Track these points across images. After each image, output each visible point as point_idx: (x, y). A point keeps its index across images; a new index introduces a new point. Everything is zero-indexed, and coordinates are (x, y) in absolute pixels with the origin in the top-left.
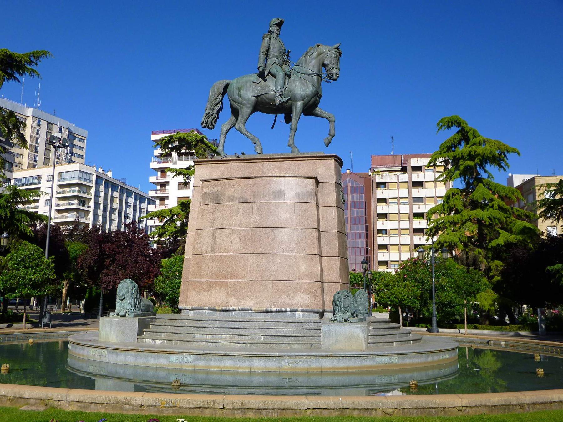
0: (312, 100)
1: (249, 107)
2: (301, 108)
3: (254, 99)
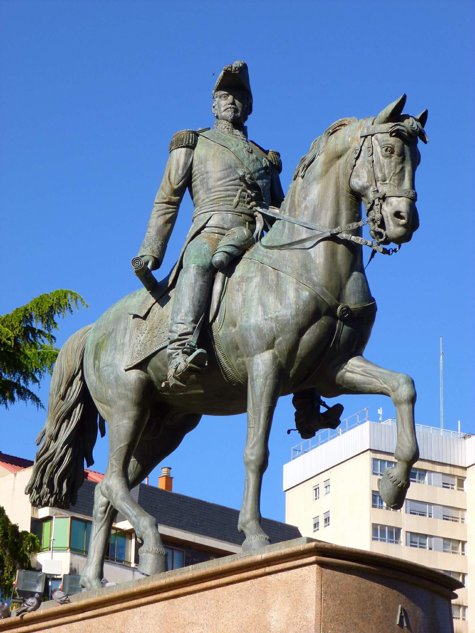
0: (306, 337)
1: (124, 410)
2: (266, 379)
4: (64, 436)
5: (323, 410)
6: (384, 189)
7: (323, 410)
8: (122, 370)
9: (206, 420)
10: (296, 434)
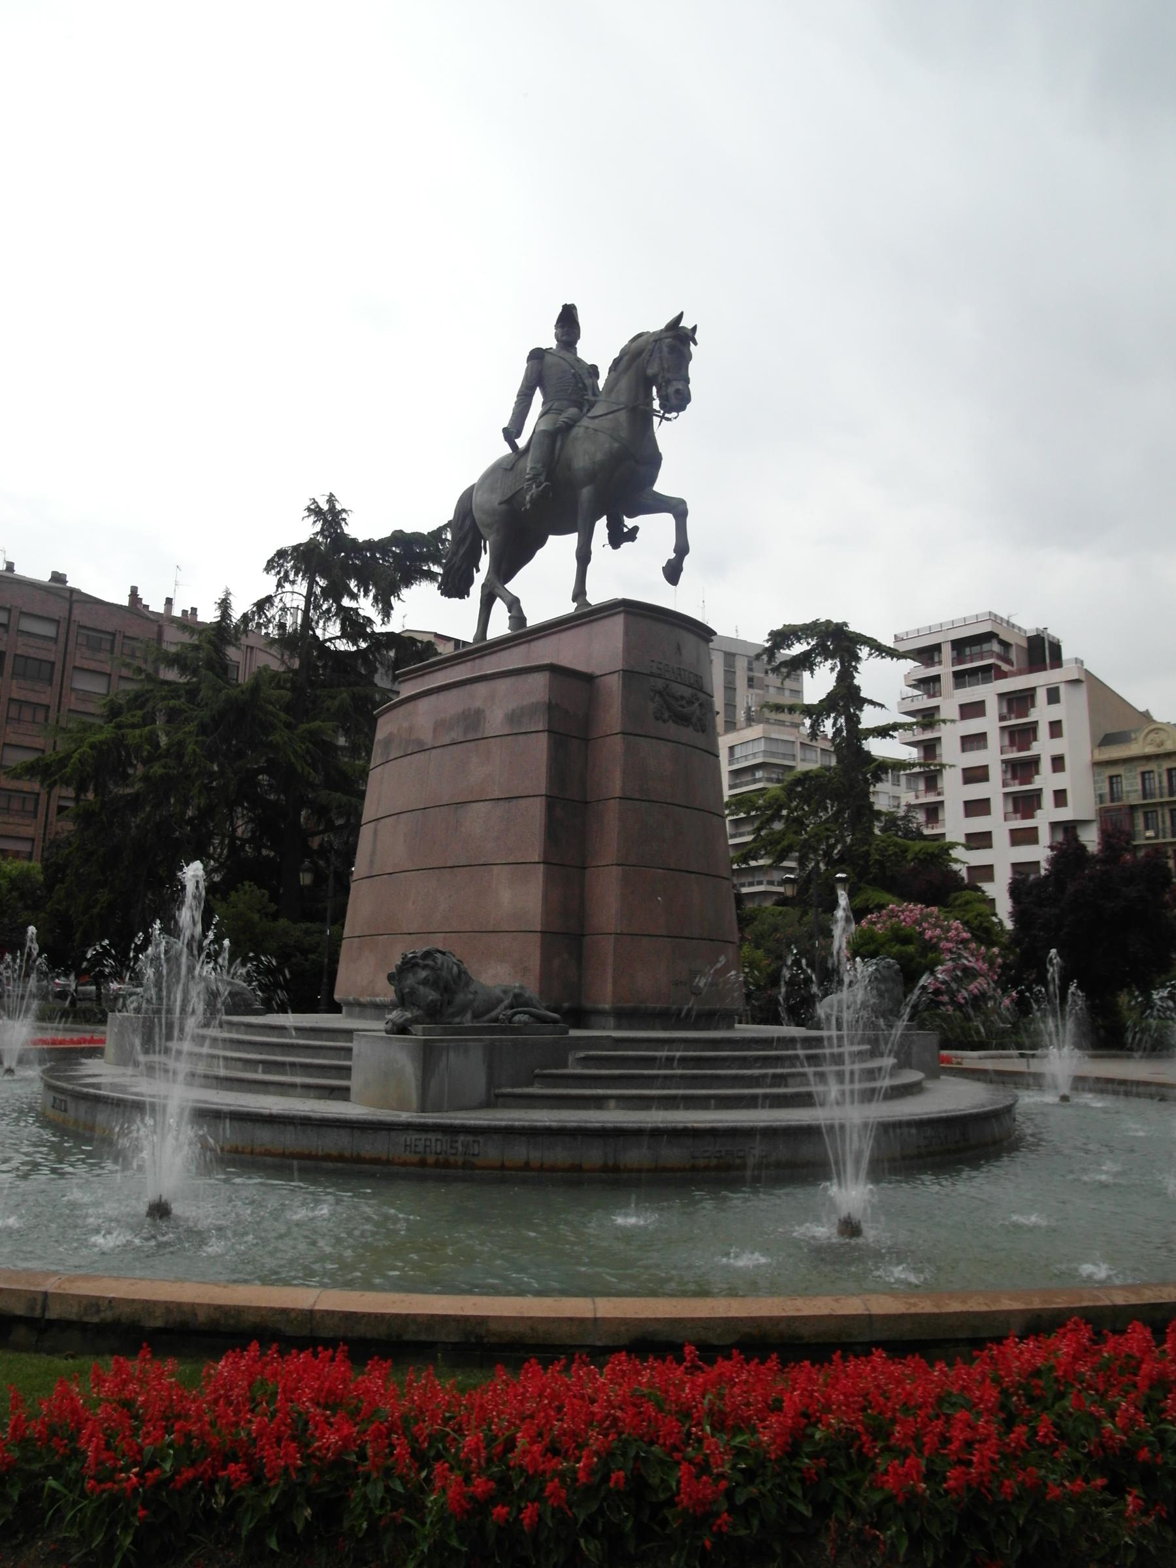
3: (503, 507)
4: (462, 552)
5: (626, 530)
6: (668, 375)
7: (626, 530)
8: (496, 503)
9: (552, 539)
10: (610, 547)
